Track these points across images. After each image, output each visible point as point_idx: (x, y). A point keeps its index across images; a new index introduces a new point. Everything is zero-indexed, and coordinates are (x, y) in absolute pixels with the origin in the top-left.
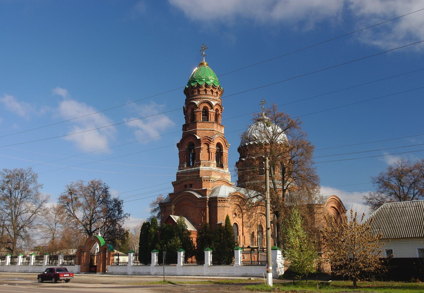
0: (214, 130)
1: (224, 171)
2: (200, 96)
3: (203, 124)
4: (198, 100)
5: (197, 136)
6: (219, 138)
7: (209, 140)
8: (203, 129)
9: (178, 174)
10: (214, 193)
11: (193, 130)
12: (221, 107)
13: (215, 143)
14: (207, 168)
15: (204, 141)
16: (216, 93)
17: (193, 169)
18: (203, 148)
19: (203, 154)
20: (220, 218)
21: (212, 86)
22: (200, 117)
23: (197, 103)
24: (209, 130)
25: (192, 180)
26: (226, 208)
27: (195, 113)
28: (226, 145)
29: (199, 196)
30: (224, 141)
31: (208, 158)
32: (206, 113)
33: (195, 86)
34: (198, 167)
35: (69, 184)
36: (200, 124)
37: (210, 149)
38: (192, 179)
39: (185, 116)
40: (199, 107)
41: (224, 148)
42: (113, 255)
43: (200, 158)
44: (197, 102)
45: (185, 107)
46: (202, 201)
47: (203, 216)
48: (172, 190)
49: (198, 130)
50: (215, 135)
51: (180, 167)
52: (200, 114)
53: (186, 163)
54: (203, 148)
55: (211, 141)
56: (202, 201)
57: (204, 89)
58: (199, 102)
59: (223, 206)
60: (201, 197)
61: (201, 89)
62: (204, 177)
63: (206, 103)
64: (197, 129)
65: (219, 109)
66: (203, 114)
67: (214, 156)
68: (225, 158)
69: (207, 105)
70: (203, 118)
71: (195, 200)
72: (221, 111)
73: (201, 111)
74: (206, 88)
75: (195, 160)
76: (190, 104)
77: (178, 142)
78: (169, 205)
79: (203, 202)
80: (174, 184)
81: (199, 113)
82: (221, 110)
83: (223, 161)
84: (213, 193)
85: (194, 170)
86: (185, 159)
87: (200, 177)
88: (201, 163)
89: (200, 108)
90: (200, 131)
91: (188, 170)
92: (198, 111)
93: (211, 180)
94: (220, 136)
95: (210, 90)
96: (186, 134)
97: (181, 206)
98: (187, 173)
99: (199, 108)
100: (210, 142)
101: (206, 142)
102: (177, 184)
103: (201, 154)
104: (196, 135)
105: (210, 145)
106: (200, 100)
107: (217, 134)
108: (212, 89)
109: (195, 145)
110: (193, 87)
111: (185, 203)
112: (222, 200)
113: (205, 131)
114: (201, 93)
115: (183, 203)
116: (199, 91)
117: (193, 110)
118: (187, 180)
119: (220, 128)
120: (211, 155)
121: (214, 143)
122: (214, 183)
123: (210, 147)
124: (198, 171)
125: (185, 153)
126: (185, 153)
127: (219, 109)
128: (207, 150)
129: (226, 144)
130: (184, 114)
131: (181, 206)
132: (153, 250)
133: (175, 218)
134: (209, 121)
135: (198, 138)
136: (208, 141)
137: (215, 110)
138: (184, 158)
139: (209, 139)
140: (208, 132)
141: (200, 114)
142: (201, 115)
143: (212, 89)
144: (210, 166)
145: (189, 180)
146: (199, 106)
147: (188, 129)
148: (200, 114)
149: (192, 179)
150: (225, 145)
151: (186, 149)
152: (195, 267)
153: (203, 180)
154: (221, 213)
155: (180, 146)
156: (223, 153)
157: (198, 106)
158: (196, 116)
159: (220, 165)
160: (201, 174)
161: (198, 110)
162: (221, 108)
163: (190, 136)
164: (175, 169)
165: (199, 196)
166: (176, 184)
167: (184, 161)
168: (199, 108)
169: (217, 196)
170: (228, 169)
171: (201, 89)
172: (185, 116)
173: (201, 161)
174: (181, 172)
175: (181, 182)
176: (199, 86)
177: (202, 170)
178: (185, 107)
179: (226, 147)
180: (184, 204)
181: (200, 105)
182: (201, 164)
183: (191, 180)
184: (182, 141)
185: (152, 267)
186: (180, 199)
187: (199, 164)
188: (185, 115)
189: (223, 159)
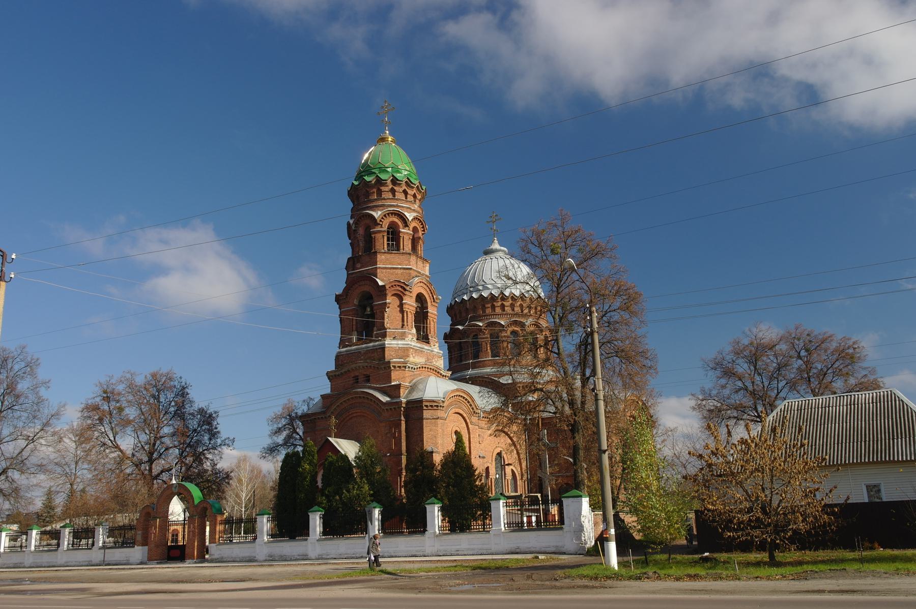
0: (411, 269)
1: (430, 348)
2: (383, 201)
3: (388, 256)
5: (377, 280)
6: (422, 284)
7: (401, 287)
8: (390, 266)
9: (338, 357)
10: (415, 392)
11: (369, 269)
12: (422, 224)
13: (414, 296)
14: (400, 342)
15: (393, 289)
16: (412, 197)
17: (371, 344)
18: (390, 304)
19: (391, 316)
20: (429, 440)
21: (406, 182)
22: (382, 242)
23: (377, 214)
24: (401, 268)
25: (370, 366)
26: (439, 421)
27: (373, 236)
28: (434, 299)
29: (384, 399)
30: (430, 290)
32: (394, 235)
33: (373, 182)
34: (381, 340)
35: (103, 380)
36: (383, 257)
37: (404, 306)
39: (350, 241)
40: (381, 223)
41: (429, 304)
42: (221, 521)
43: (386, 323)
44: (377, 214)
45: (351, 222)
46: (391, 409)
47: (394, 438)
48: (326, 388)
49: (380, 268)
50: (413, 278)
51: (342, 343)
52: (383, 236)
53: (356, 333)
54: (390, 304)
55: (405, 290)
56: (392, 407)
57: (390, 187)
58: (380, 213)
59: (435, 417)
60: (389, 401)
61: (383, 188)
62: (394, 360)
63: (395, 216)
64: (378, 266)
65: (418, 227)
66: (388, 237)
67: (411, 318)
68: (432, 323)
69: (396, 219)
70: (388, 244)
72: (423, 232)
73: (384, 231)
74: (394, 187)
75: (374, 327)
76: (363, 216)
77: (339, 291)
78: (322, 418)
79: (394, 410)
80: (331, 376)
82: (423, 229)
84: (413, 392)
85: (373, 346)
86: (354, 327)
87: (386, 360)
88: (387, 333)
89: (383, 226)
92: (380, 232)
94: (423, 281)
95: (401, 190)
96: (353, 276)
97: (348, 418)
98: (357, 354)
99: (382, 225)
100: (404, 292)
101: (396, 292)
102: (338, 375)
103: (386, 315)
104: (377, 277)
105: (404, 298)
106: (383, 210)
107: (416, 276)
108: (406, 188)
109: (374, 297)
110: (367, 184)
111: (356, 413)
112: (432, 406)
113: (394, 271)
114: (383, 196)
115: (352, 414)
116: (380, 193)
117: (368, 228)
119: (422, 265)
120: (407, 317)
121: (411, 295)
123: (403, 301)
124: (383, 348)
127: (419, 229)
128: (398, 307)
129: (433, 296)
131: (348, 418)
132: (567, 491)
133: (337, 443)
134: (402, 251)
135: (381, 283)
136: (400, 289)
137: (411, 229)
139: (403, 285)
142: (386, 238)
143: (406, 188)
144: (404, 339)
146: (381, 221)
147: (358, 265)
148: (383, 236)
150: (432, 298)
152: (405, 538)
153: (393, 366)
154: (430, 431)
156: (429, 314)
157: (378, 221)
158: (375, 241)
159: (423, 337)
160: (388, 355)
161: (378, 228)
162: (422, 226)
163: (364, 280)
164: (334, 348)
165: (384, 399)
166: (335, 376)
168: (380, 224)
169: (422, 398)
170: (437, 345)
171: (383, 188)
172: (350, 241)
173: (386, 329)
174: (346, 351)
175: (345, 372)
176: (380, 182)
177: (389, 347)
178: (351, 222)
179: (434, 301)
180: (355, 415)
181: (382, 218)
183: (367, 366)
184: (346, 290)
186: (346, 405)
187: (384, 336)
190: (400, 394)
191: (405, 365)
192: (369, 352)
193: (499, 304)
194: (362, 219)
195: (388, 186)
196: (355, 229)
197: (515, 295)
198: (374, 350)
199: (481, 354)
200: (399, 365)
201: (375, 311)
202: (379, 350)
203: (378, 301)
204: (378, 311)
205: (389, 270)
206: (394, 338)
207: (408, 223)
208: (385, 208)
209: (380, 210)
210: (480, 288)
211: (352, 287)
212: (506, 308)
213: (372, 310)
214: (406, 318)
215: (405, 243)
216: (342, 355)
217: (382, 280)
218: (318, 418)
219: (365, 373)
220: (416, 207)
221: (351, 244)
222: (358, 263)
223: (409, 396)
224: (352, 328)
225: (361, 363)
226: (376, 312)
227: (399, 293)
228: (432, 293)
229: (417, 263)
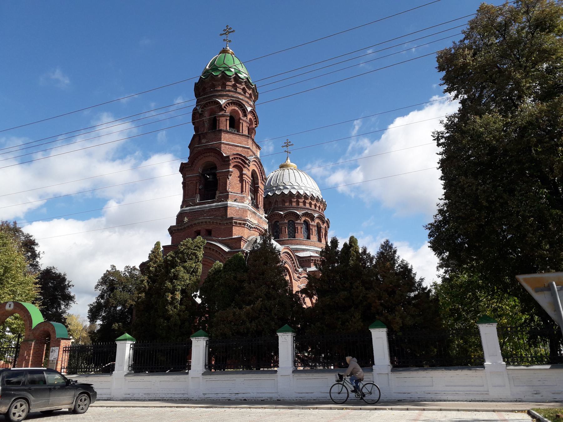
0: (249, 148)
4: (223, 99)
6: (255, 163)
7: (242, 160)
11: (213, 144)
14: (240, 204)
15: (235, 160)
18: (232, 172)
23: (222, 102)
24: (241, 147)
25: (213, 222)
28: (262, 178)
29: (226, 249)
30: (261, 171)
31: (240, 190)
33: (219, 76)
34: (223, 201)
37: (244, 176)
38: (211, 221)
40: (225, 109)
41: (260, 181)
44: (222, 101)
49: (224, 143)
52: (226, 120)
53: (199, 195)
54: (232, 172)
55: (246, 163)
58: (224, 101)
67: (248, 187)
68: (260, 197)
71: (219, 256)
72: (255, 125)
73: (227, 116)
75: (217, 190)
81: (225, 118)
82: (255, 123)
83: (258, 200)
88: (229, 196)
89: (227, 112)
91: (205, 206)
92: (223, 116)
93: (246, 224)
94: (257, 161)
99: (225, 111)
102: (181, 229)
103: (228, 181)
105: (244, 169)
114: (227, 89)
116: (224, 86)
117: (212, 112)
118: (202, 222)
120: (246, 185)
121: (249, 168)
122: (250, 230)
124: (226, 207)
125: (197, 180)
126: (197, 180)
128: (239, 177)
129: (262, 176)
135: (224, 155)
138: (195, 188)
141: (226, 122)
144: (243, 202)
145: (205, 222)
148: (226, 120)
149: (211, 221)
151: (199, 173)
153: (235, 222)
155: (188, 167)
157: (223, 107)
158: (219, 123)
160: (230, 213)
161: (222, 113)
163: (209, 152)
165: (226, 249)
166: (178, 230)
167: (195, 192)
168: (224, 110)
173: (228, 192)
174: (189, 210)
176: (225, 78)
181: (226, 105)
182: (229, 198)
183: (209, 222)
187: (226, 198)
189: (259, 198)
190: (241, 245)
191: (245, 222)
192: (212, 211)
193: (295, 200)
194: (209, 104)
195: (231, 82)
196: (201, 113)
198: (217, 209)
199: (281, 235)
200: (240, 222)
201: (218, 178)
202: (221, 209)
203: (223, 170)
204: (221, 177)
206: (235, 200)
207: (247, 113)
208: (229, 98)
209: (224, 99)
210: (282, 187)
211: (197, 158)
212: (300, 204)
214: (244, 185)
215: (244, 129)
216: (186, 212)
217: (225, 154)
219: (207, 228)
220: (252, 104)
221: (195, 128)
222: (203, 138)
224: (196, 191)
225: (201, 219)
226: (219, 178)
228: (261, 173)
229: (252, 146)
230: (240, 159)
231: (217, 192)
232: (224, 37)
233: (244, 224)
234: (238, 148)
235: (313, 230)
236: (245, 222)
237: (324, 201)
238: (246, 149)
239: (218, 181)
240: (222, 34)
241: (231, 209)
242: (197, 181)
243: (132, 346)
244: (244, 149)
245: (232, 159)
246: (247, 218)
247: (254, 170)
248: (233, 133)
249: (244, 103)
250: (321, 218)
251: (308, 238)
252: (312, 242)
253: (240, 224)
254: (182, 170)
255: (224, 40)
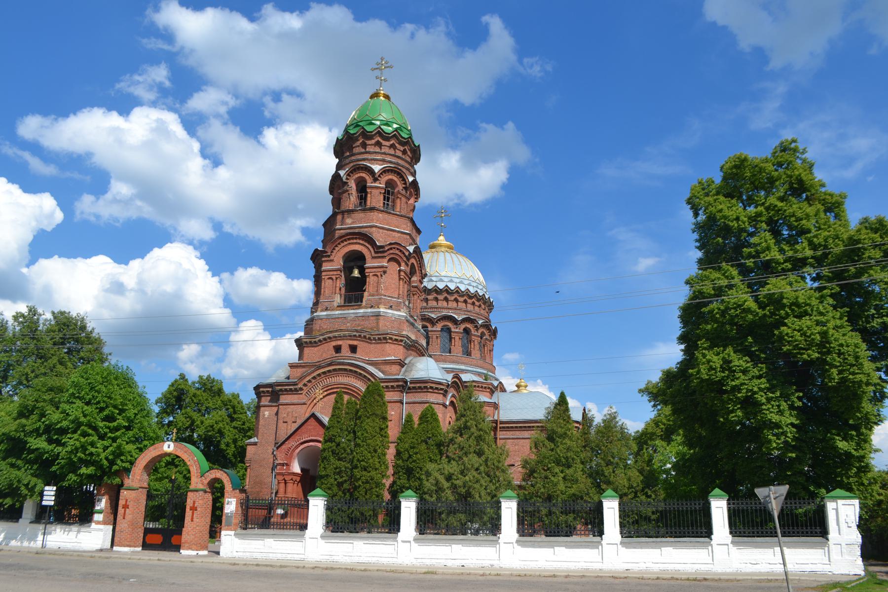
15: (391, 252)
17: (362, 311)
24: (398, 232)
27: (368, 190)
36: (380, 215)
39: (332, 196)
54: (386, 268)
90: (381, 231)
106: (382, 165)
109: (367, 258)
113: (391, 233)
130: (329, 192)
136: (399, 253)
139: (402, 249)
140: (396, 236)
146: (379, 176)
166: (311, 342)
185: (403, 542)
188: (331, 194)
191: (403, 339)
197: (470, 292)
200: (397, 338)
202: (372, 318)
205: (386, 231)
206: (391, 307)
211: (339, 244)
213: (362, 270)
218: (286, 390)
222: (348, 217)
223: (406, 374)
224: (336, 290)
227: (397, 257)
230: (398, 249)
231: (366, 294)
232: (377, 73)
233: (401, 341)
234: (394, 233)
235: (476, 343)
236: (403, 339)
237: (492, 300)
238: (405, 236)
239: (368, 279)
240: (375, 69)
241: (384, 319)
242: (337, 276)
243: (326, 503)
244: (402, 235)
245: (388, 250)
246: (404, 333)
247: (413, 264)
248: (390, 213)
249: (404, 170)
250: (487, 326)
251: (468, 353)
252: (474, 360)
253: (396, 340)
254: (316, 258)
255: (377, 78)
